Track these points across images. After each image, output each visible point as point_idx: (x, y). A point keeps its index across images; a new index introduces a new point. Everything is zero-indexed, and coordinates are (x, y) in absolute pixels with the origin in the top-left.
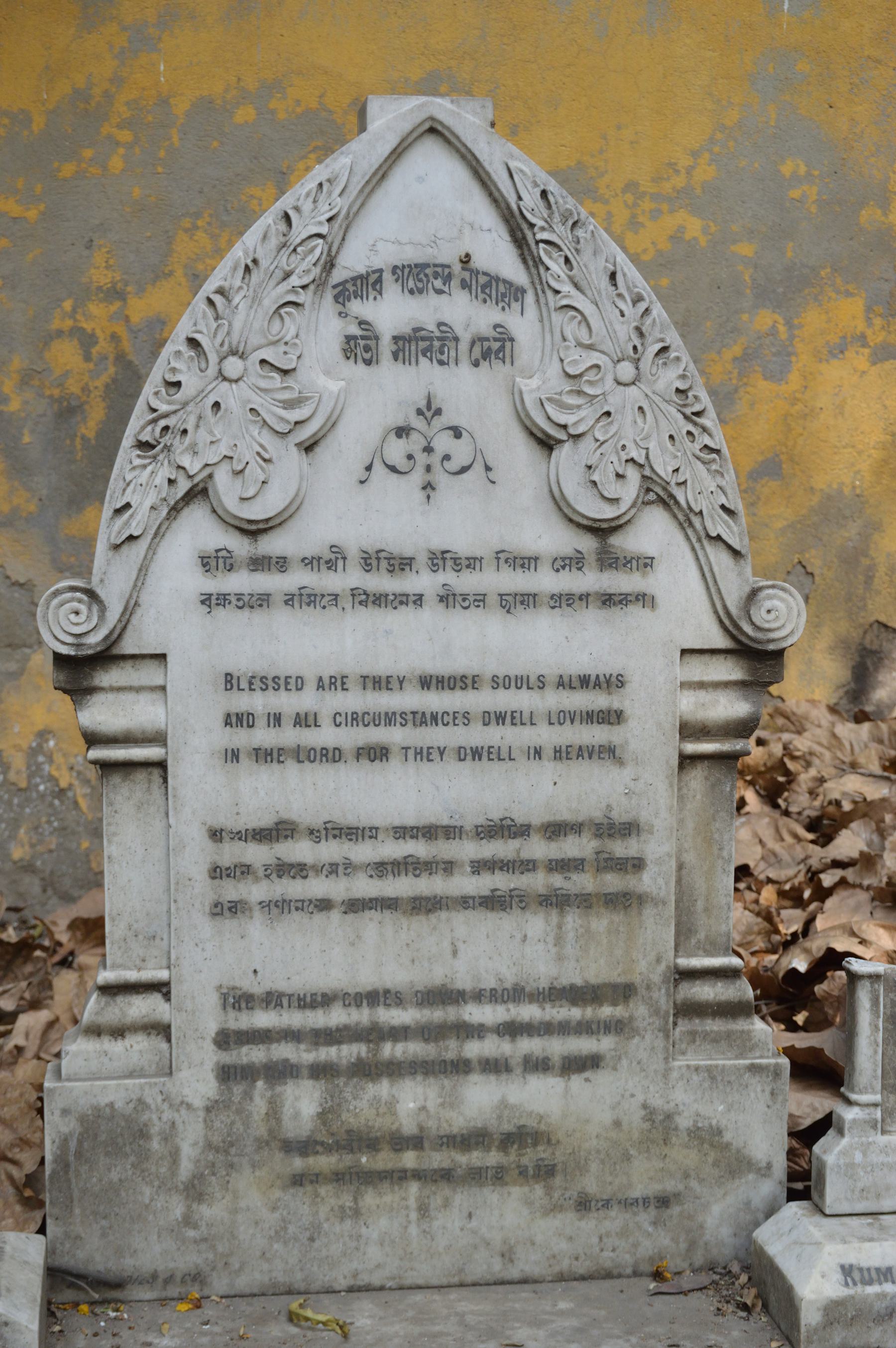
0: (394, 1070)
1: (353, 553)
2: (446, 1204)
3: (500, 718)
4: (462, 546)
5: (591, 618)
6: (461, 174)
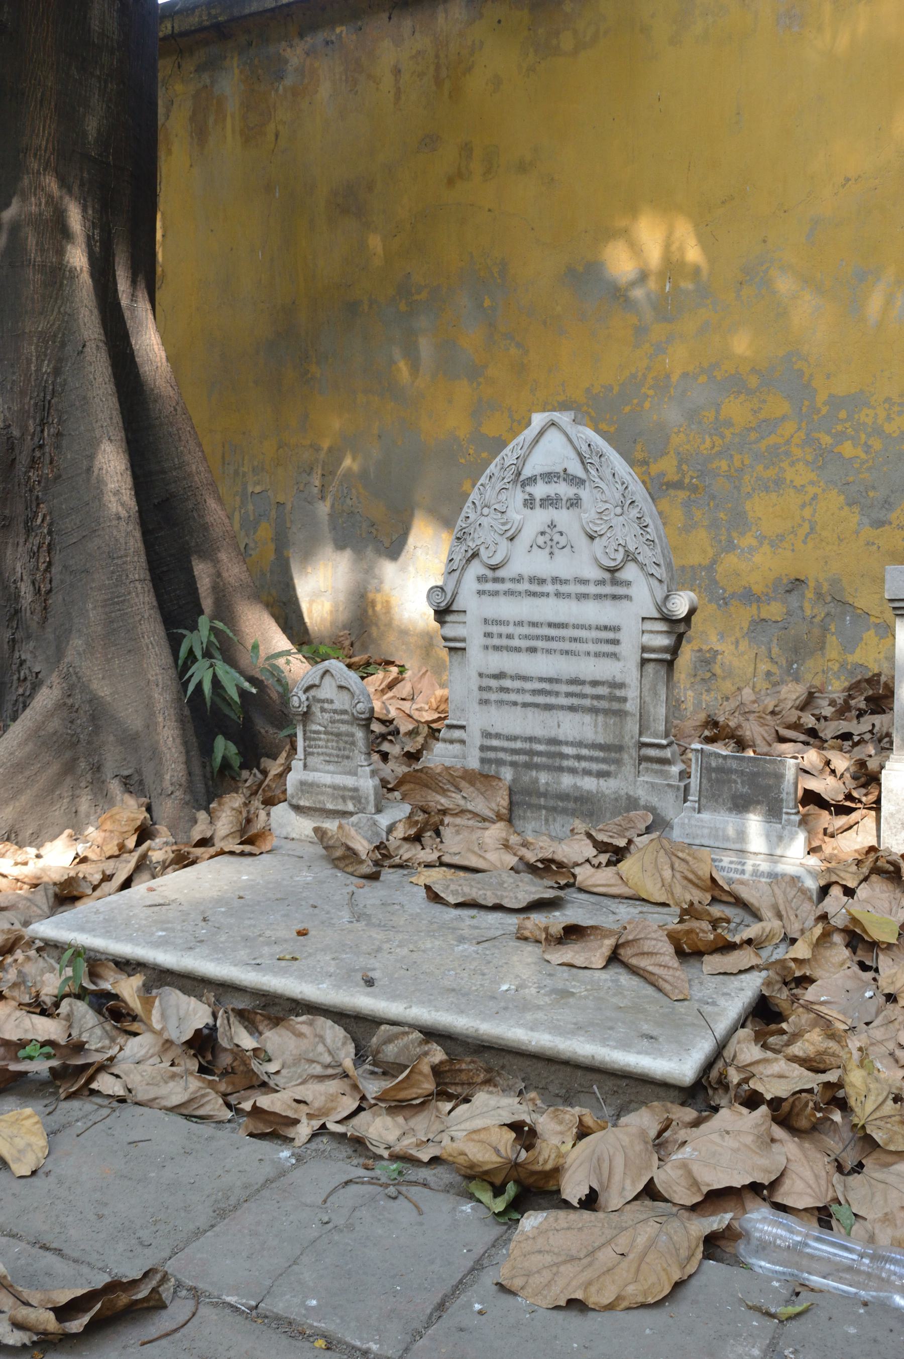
0: (538, 767)
1: (526, 577)
2: (554, 820)
3: (575, 640)
4: (564, 575)
5: (608, 603)
6: (564, 439)
